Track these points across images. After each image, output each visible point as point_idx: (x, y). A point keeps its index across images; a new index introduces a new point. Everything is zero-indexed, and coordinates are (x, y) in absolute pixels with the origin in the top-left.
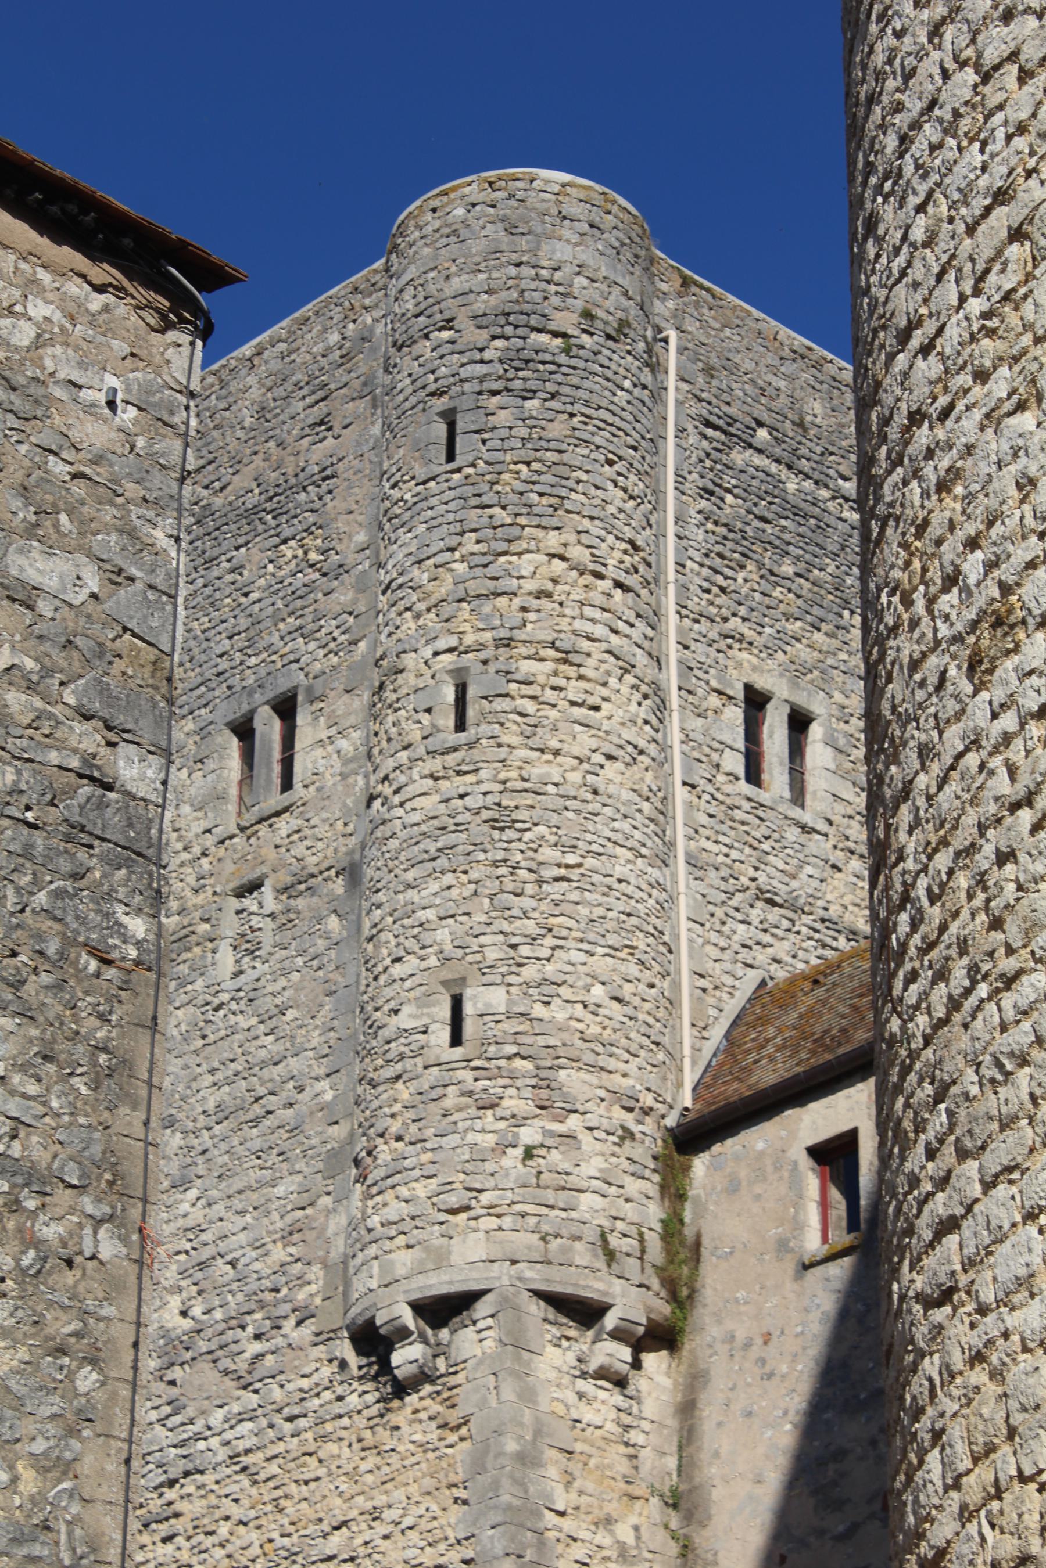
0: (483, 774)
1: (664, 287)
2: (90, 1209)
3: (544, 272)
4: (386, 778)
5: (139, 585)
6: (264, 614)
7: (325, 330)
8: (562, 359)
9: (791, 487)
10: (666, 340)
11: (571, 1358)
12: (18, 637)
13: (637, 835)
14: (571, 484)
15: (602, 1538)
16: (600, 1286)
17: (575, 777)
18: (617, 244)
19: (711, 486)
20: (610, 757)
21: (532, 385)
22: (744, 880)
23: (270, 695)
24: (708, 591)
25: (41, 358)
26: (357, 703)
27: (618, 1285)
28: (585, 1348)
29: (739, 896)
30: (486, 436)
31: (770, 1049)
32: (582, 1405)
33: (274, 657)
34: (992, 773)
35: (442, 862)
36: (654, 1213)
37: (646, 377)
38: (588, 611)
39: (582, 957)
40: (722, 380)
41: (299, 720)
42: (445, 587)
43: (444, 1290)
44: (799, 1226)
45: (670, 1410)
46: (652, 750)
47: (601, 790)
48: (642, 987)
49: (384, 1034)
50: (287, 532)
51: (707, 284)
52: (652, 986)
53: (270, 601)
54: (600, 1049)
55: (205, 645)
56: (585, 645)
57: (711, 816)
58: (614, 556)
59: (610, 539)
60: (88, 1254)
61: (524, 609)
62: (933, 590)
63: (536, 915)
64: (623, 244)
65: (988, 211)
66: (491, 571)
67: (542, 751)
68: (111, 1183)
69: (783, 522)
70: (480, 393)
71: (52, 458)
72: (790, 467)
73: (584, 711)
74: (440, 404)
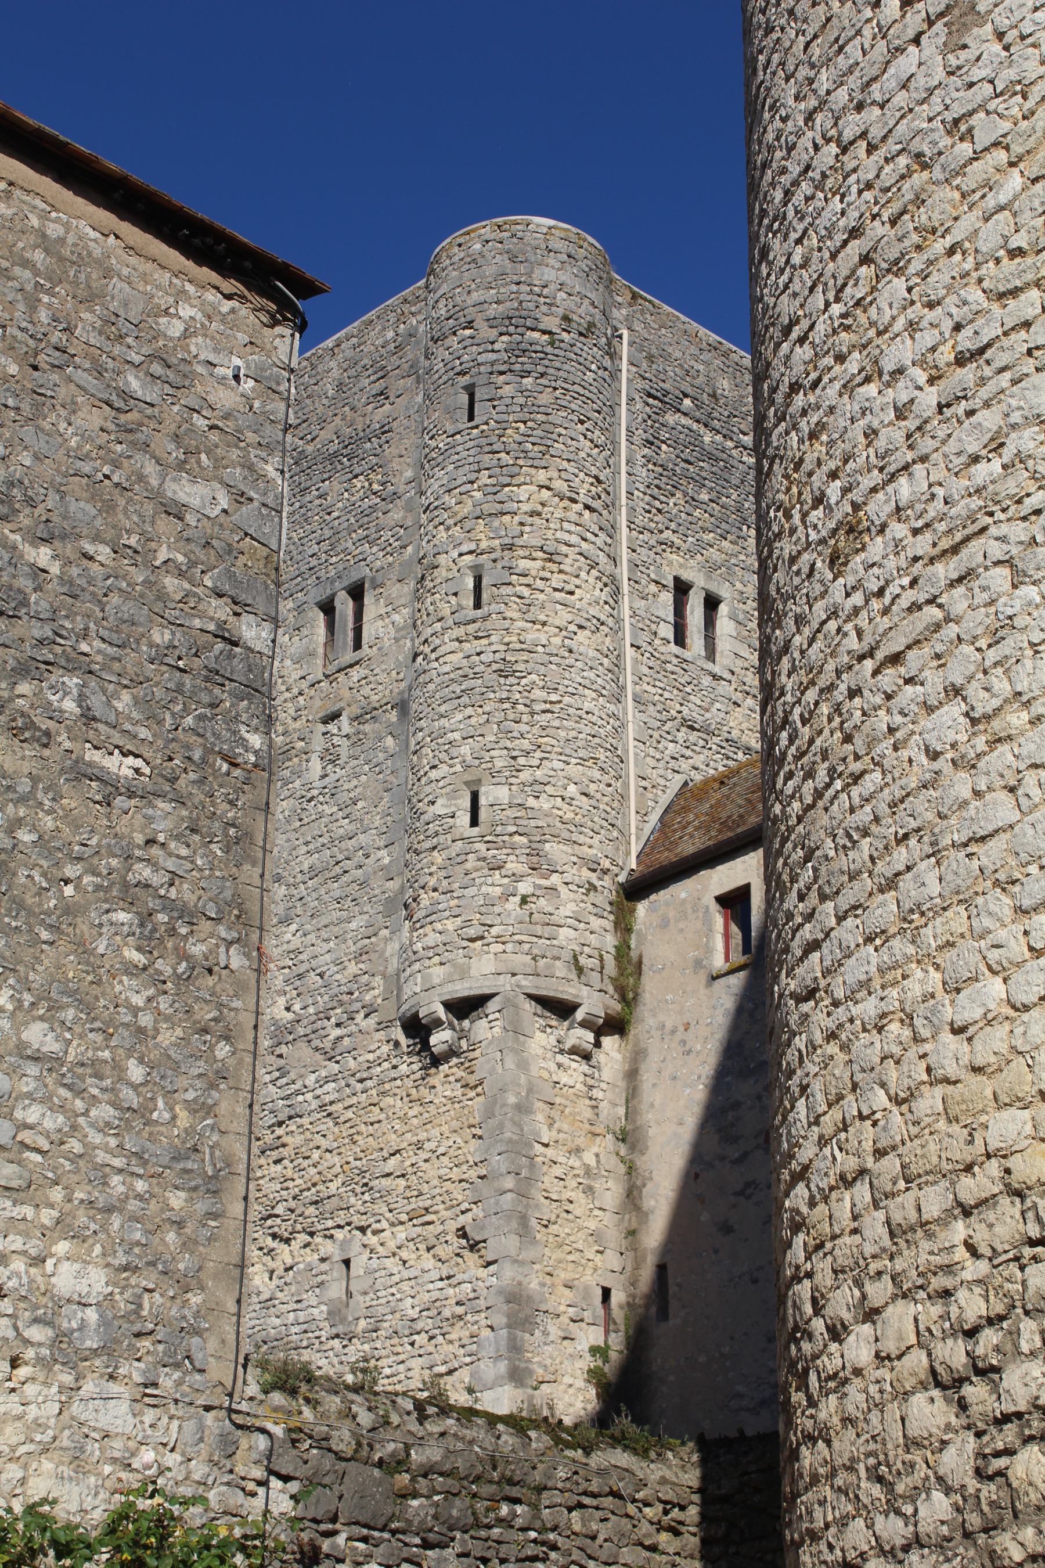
0: (493, 639)
1: (619, 299)
2: (223, 934)
4: (426, 641)
5: (256, 504)
6: (342, 527)
7: (384, 329)
8: (549, 349)
9: (707, 439)
10: (620, 337)
11: (553, 1040)
12: (172, 540)
13: (599, 681)
14: (554, 436)
15: (574, 1161)
17: (557, 641)
19: (651, 438)
20: (580, 627)
21: (527, 367)
22: (673, 713)
23: (346, 583)
24: (649, 512)
25: (188, 345)
26: (406, 589)
27: (585, 991)
28: (562, 1033)
29: (669, 724)
31: (690, 829)
32: (560, 1072)
34: (846, 634)
35: (465, 700)
36: (610, 941)
37: (607, 362)
38: (566, 525)
39: (561, 765)
40: (660, 365)
41: (366, 601)
42: (467, 509)
43: (466, 993)
44: (709, 950)
45: (621, 1075)
46: (610, 622)
47: (575, 649)
48: (602, 786)
49: (425, 818)
50: (357, 470)
51: (649, 297)
52: (609, 785)
53: (345, 518)
54: (573, 829)
55: (301, 548)
56: (564, 549)
58: (584, 489)
59: (582, 475)
60: (222, 965)
61: (522, 524)
62: (806, 507)
63: (529, 736)
65: (845, 243)
66: (499, 497)
67: (534, 622)
68: (238, 917)
69: (701, 464)
70: (491, 373)
71: (195, 415)
72: (706, 426)
73: (563, 595)
74: (465, 380)
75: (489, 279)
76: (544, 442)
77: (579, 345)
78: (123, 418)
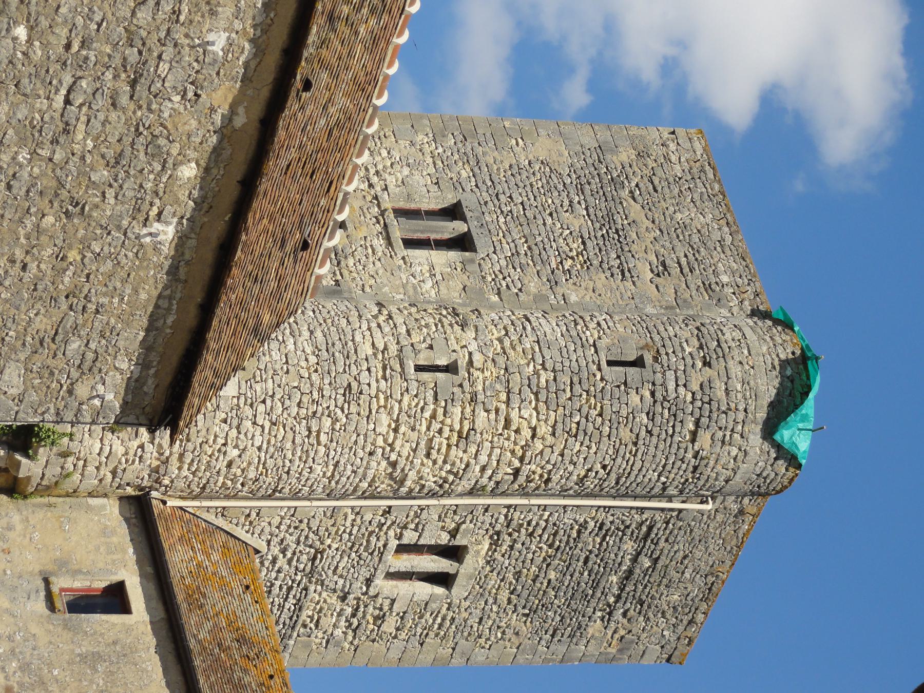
3: (740, 427)
4: (390, 317)
5: (16, 408)
7: (733, 273)
13: (344, 479)
14: (587, 442)
18: (764, 474)
19: (605, 528)
21: (658, 419)
22: (329, 541)
24: (529, 523)
33: (501, 234)
46: (404, 490)
50: (589, 244)
56: (473, 449)
57: (370, 522)
63: (285, 416)
64: (765, 478)
69: (586, 573)
70: (653, 384)
75: (752, 383)
76: (581, 433)
77: (684, 466)
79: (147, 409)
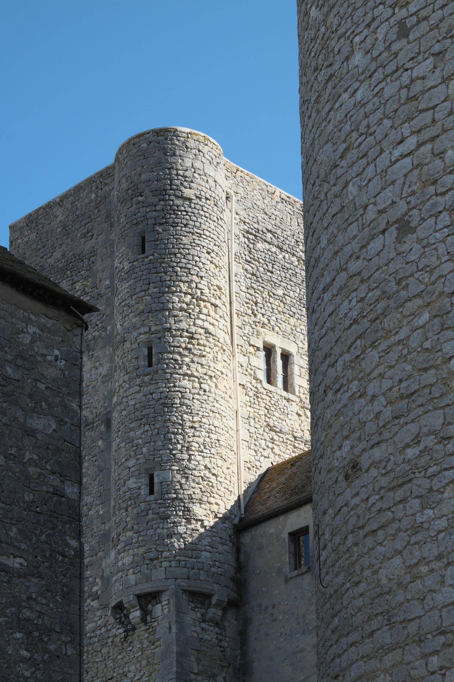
2: (64, 639)
5: (69, 425)
11: (199, 614)
12: (31, 448)
16: (209, 587)
25: (33, 347)
27: (216, 587)
30: (158, 243)
35: (144, 420)
43: (149, 590)
49: (123, 489)
60: (64, 654)
62: (334, 449)
68: (70, 630)
78: (5, 389)
79: (68, 327)
